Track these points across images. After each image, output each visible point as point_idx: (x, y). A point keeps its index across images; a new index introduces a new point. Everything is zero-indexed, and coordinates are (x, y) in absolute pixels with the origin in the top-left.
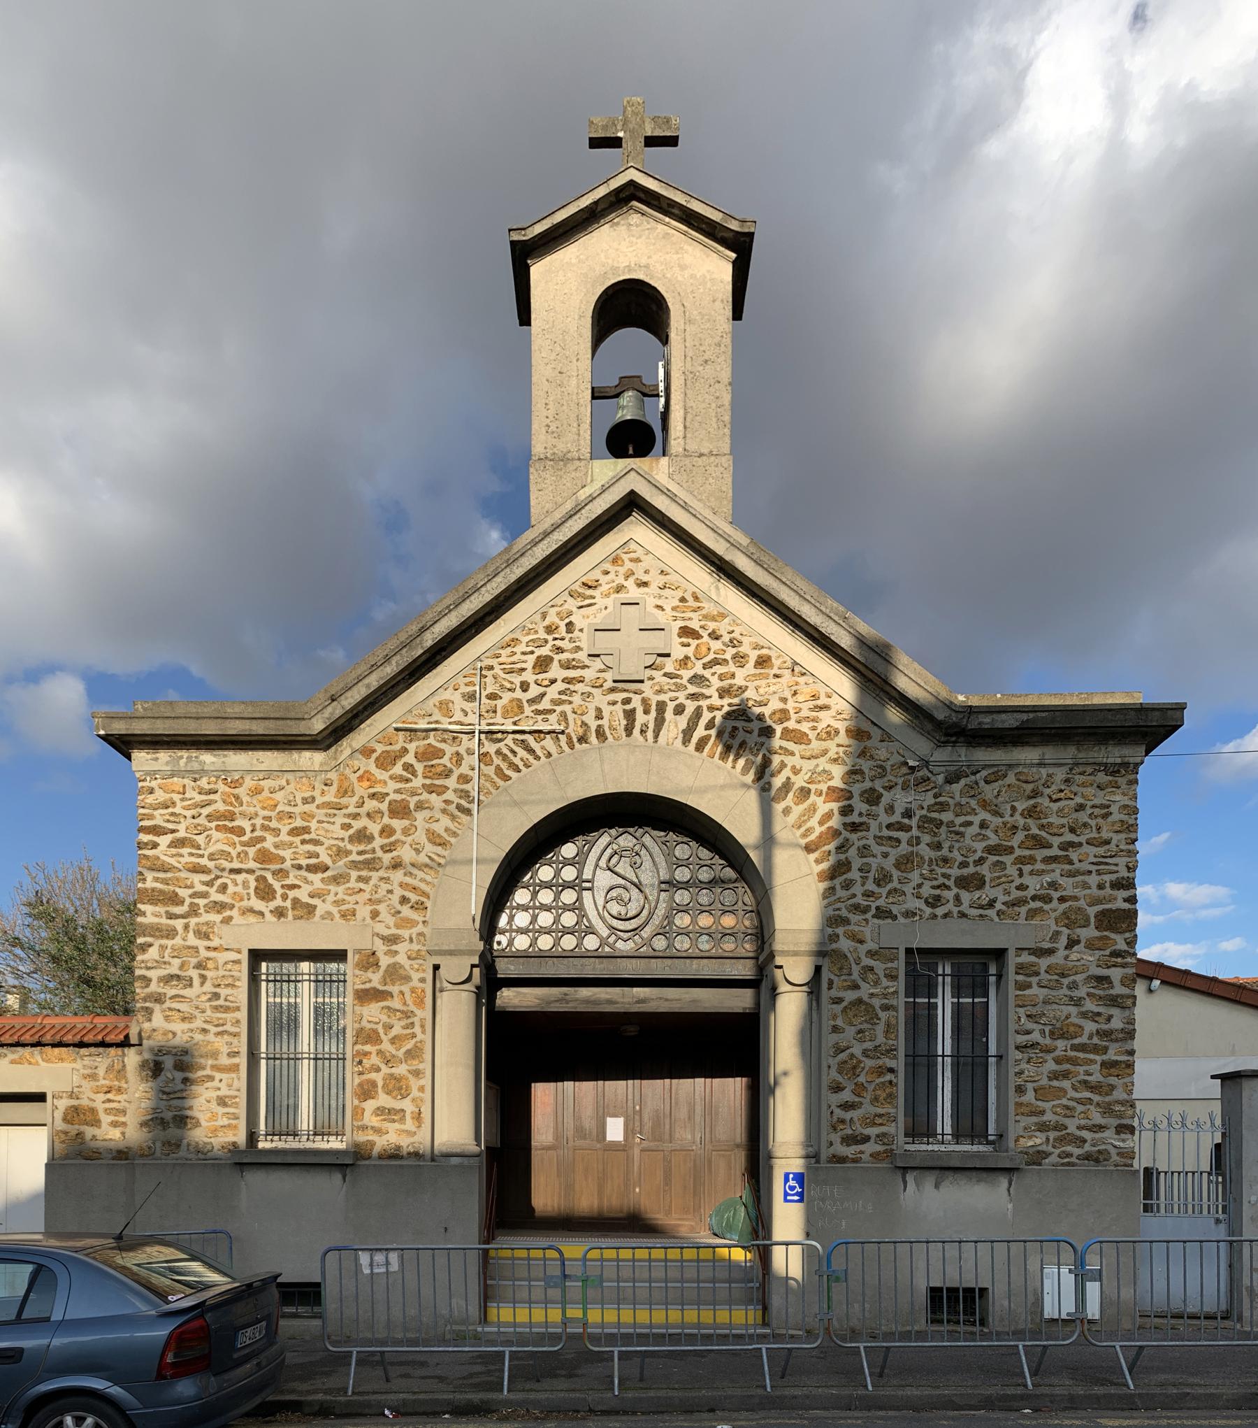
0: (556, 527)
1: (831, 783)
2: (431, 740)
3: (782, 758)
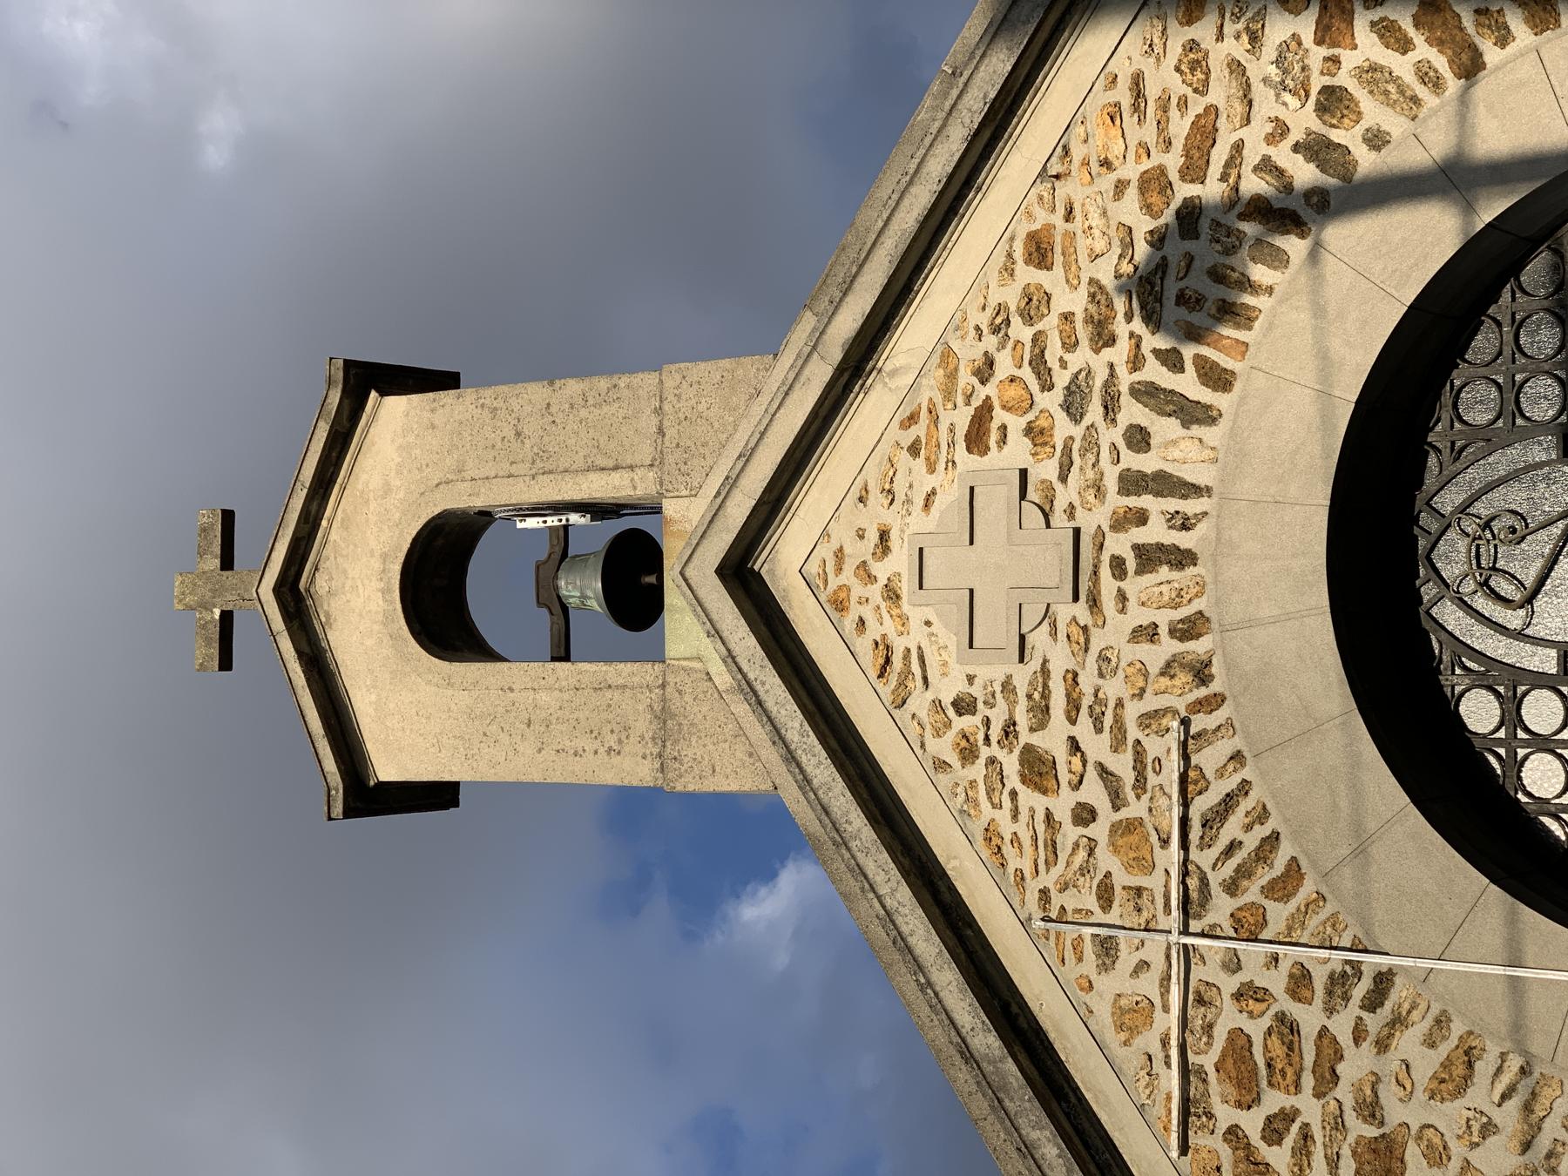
0: (778, 735)
1: (1308, 37)
2: (1207, 1060)
3: (1247, 170)
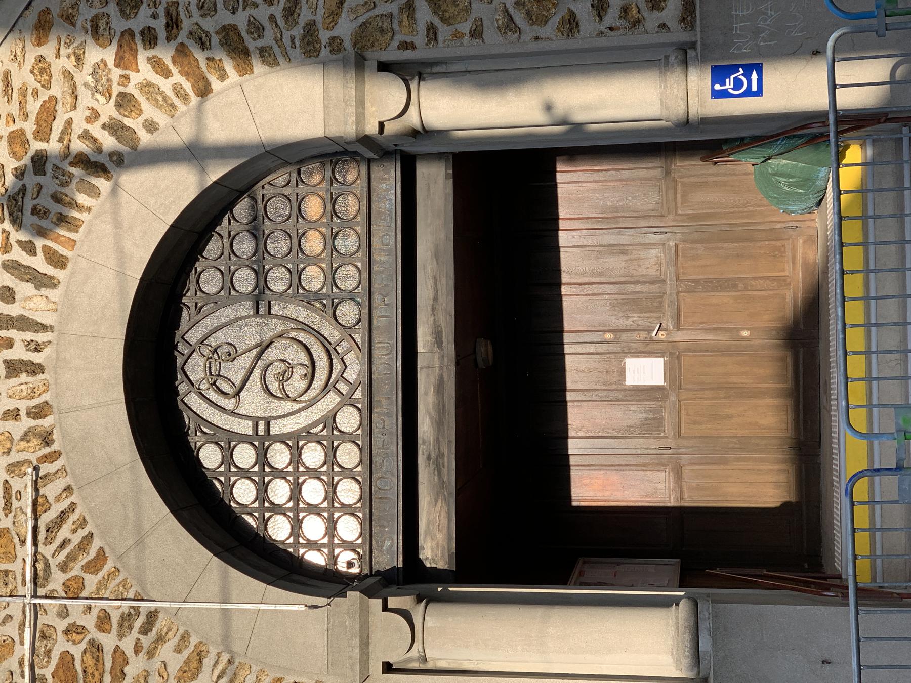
1: (111, 62)
2: (48, 672)
3: (74, 137)
